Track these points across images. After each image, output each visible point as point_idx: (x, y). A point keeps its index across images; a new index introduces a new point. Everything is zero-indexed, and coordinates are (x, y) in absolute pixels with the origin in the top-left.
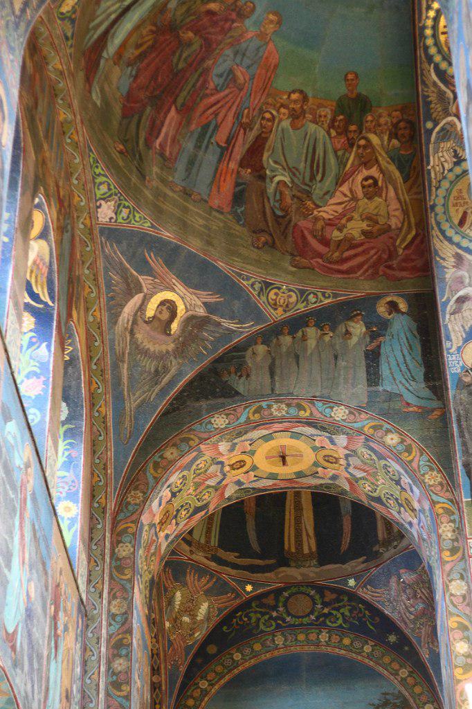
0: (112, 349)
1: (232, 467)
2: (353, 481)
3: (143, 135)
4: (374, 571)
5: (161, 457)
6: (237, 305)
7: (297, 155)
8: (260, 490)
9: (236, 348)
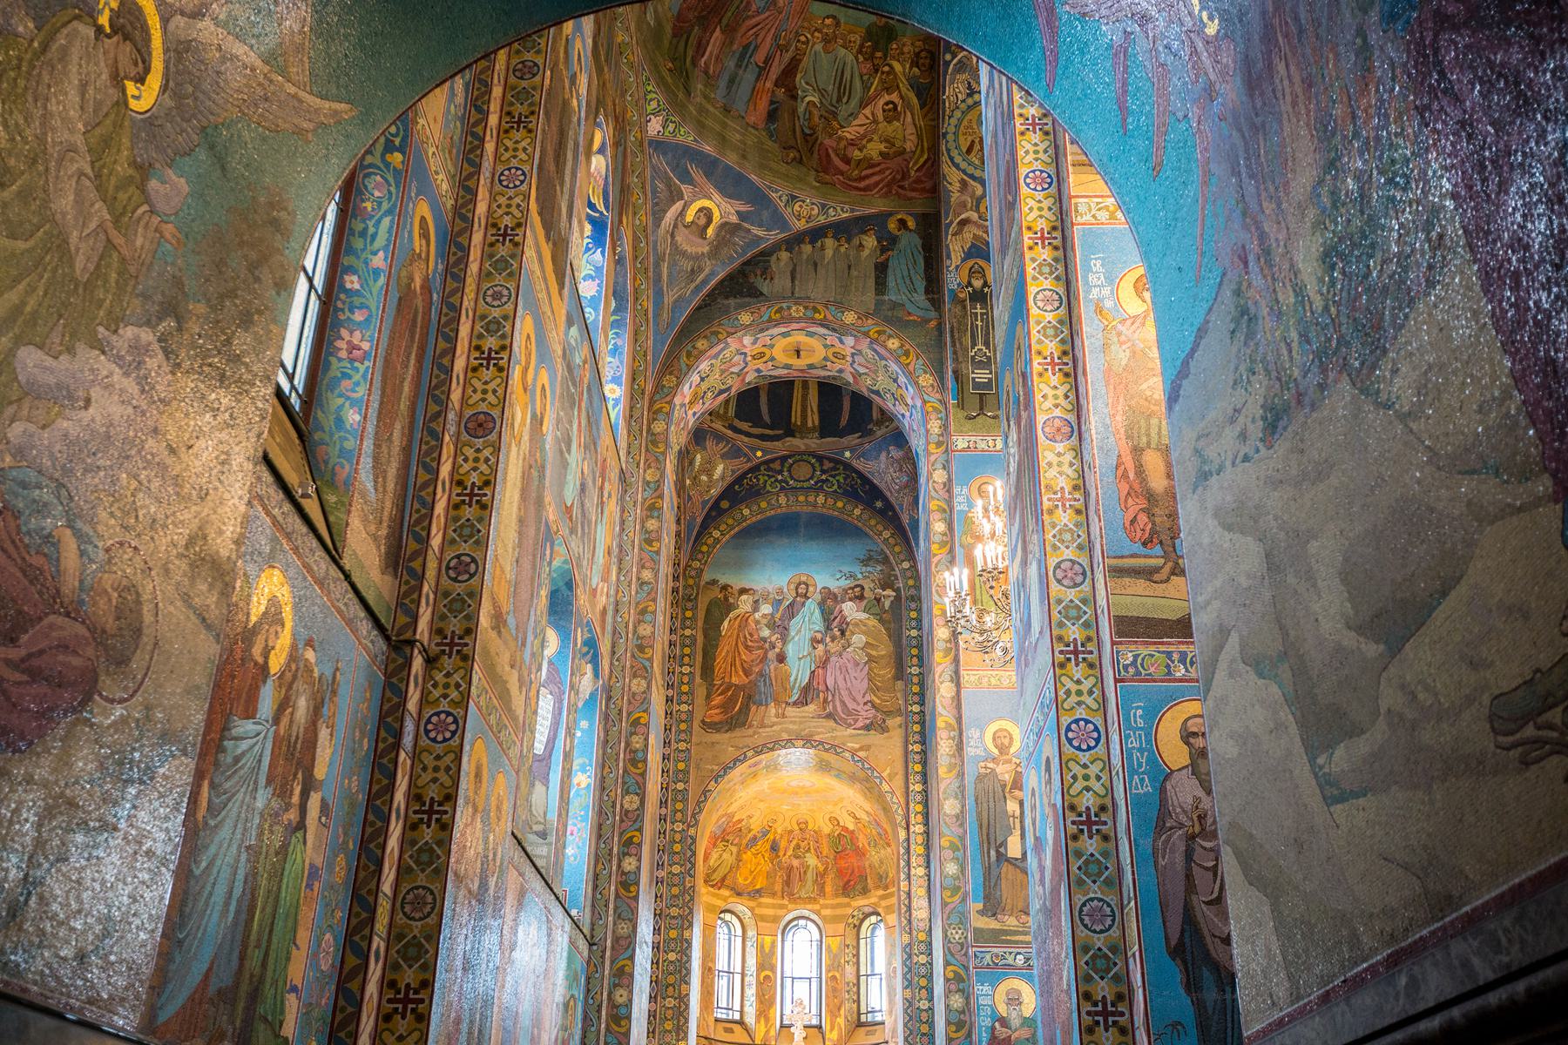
0: (655, 248)
3: (690, 53)
4: (867, 446)
5: (694, 347)
6: (765, 214)
7: (827, 79)
8: (776, 377)
9: (762, 253)
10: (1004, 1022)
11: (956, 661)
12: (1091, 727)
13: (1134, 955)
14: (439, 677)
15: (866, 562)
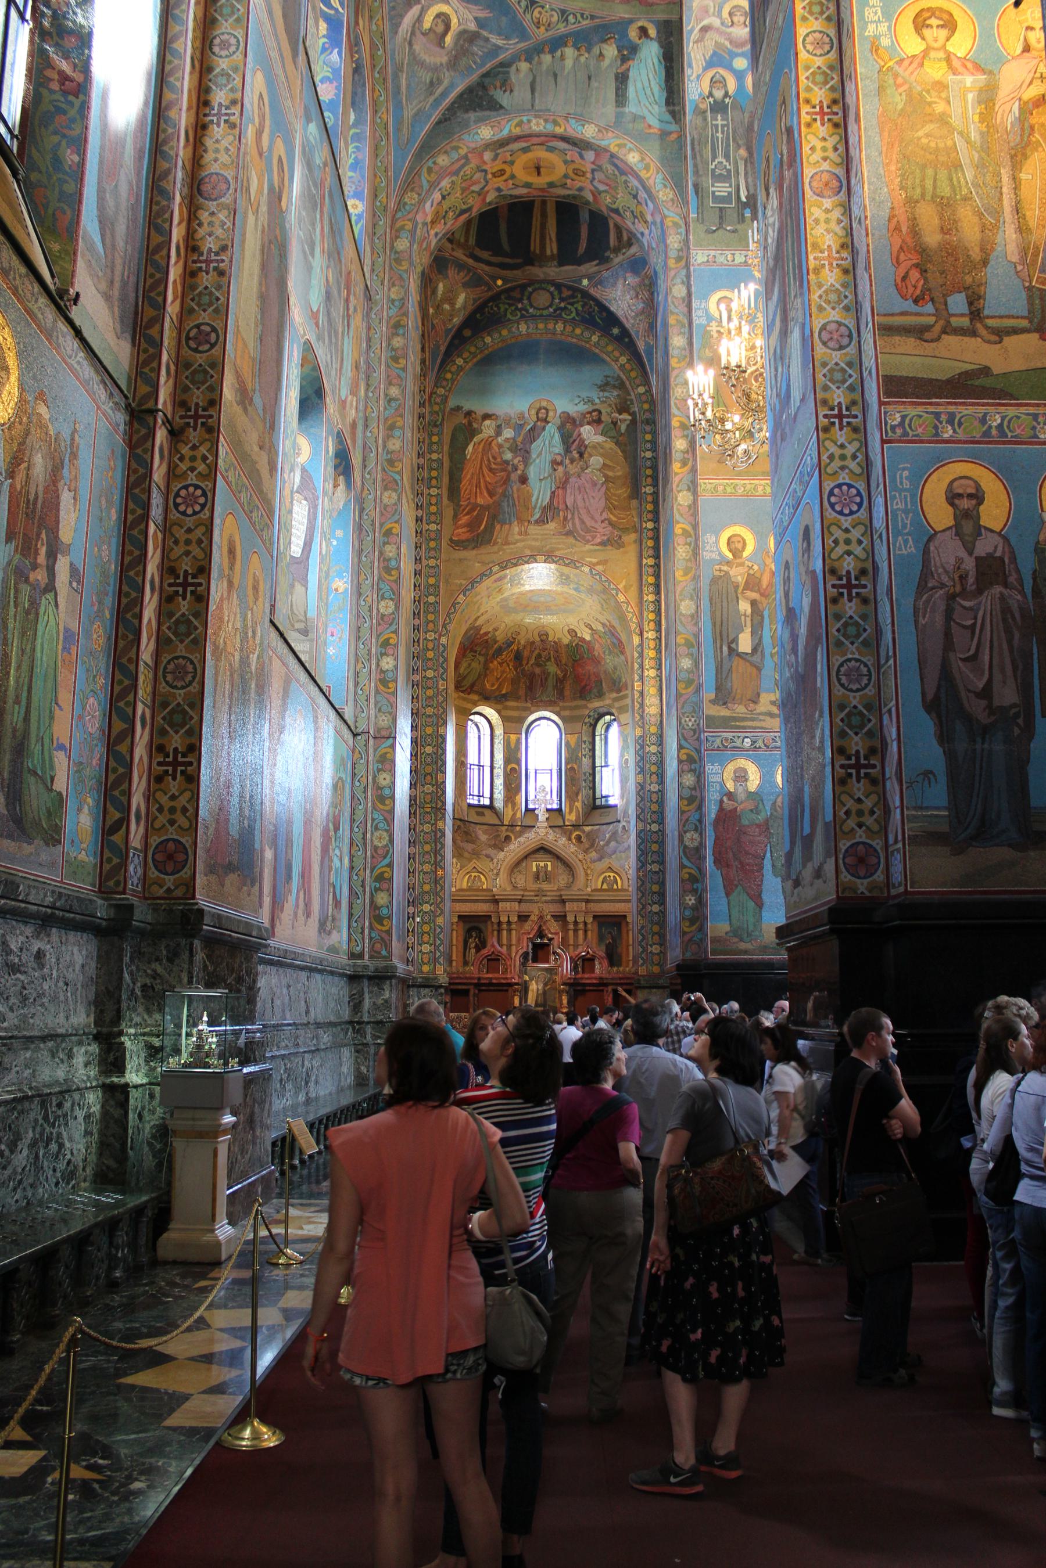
0: (393, 58)
1: (494, 175)
2: (596, 194)
4: (605, 274)
5: (434, 163)
8: (516, 197)
9: (502, 65)
10: (730, 795)
11: (694, 471)
12: (853, 491)
13: (889, 711)
14: (185, 450)
15: (603, 387)
